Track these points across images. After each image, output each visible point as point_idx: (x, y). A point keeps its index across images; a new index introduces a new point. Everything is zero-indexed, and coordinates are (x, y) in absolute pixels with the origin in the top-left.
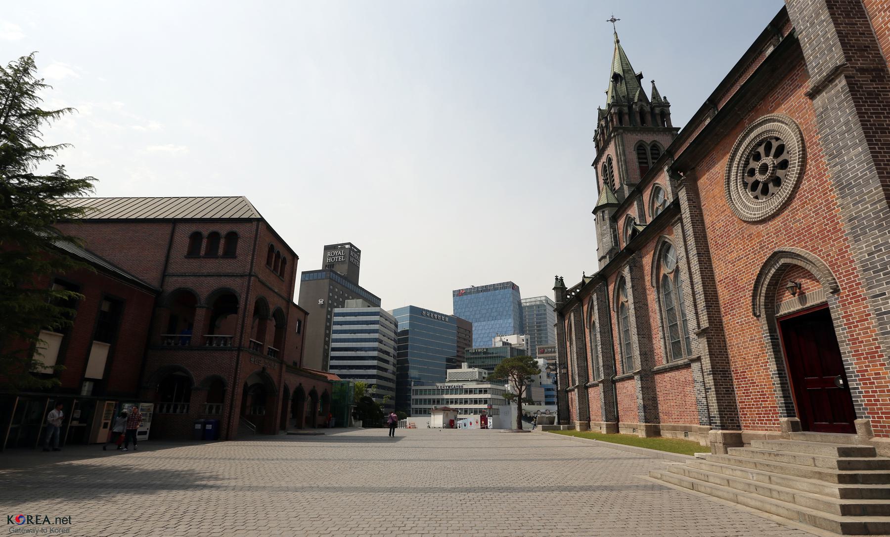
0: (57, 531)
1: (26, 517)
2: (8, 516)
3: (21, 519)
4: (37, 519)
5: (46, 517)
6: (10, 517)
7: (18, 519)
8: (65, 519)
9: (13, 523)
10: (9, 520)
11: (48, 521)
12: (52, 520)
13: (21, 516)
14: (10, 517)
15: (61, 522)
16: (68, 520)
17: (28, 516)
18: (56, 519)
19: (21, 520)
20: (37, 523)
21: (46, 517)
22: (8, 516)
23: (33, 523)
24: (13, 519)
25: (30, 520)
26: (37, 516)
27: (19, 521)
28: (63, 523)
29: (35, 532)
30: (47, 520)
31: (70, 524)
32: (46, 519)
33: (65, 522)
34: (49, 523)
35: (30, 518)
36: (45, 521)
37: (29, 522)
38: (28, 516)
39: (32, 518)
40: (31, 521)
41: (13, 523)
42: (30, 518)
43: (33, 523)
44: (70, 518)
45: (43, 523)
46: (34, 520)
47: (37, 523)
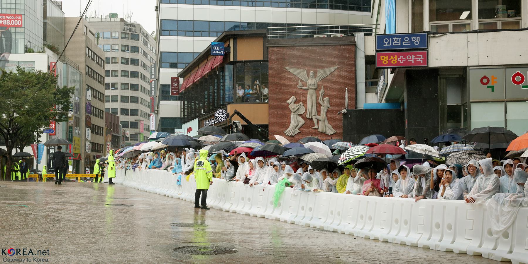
0: (38, 260)
2: (2, 249)
3: (11, 251)
4: (24, 252)
5: (31, 250)
6: (4, 250)
7: (9, 252)
9: (6, 255)
10: (3, 252)
11: (32, 252)
12: (35, 252)
13: (12, 249)
14: (4, 250)
15: (42, 254)
16: (47, 252)
18: (38, 251)
19: (12, 252)
20: (24, 254)
21: (31, 250)
22: (2, 249)
23: (21, 255)
24: (6, 251)
27: (10, 253)
28: (43, 255)
29: (23, 261)
32: (31, 252)
33: (44, 254)
34: (33, 255)
35: (18, 250)
36: (30, 252)
37: (18, 254)
38: (17, 249)
39: (20, 250)
41: (6, 255)
42: (18, 250)
44: (48, 251)
45: (28, 255)
46: (21, 252)
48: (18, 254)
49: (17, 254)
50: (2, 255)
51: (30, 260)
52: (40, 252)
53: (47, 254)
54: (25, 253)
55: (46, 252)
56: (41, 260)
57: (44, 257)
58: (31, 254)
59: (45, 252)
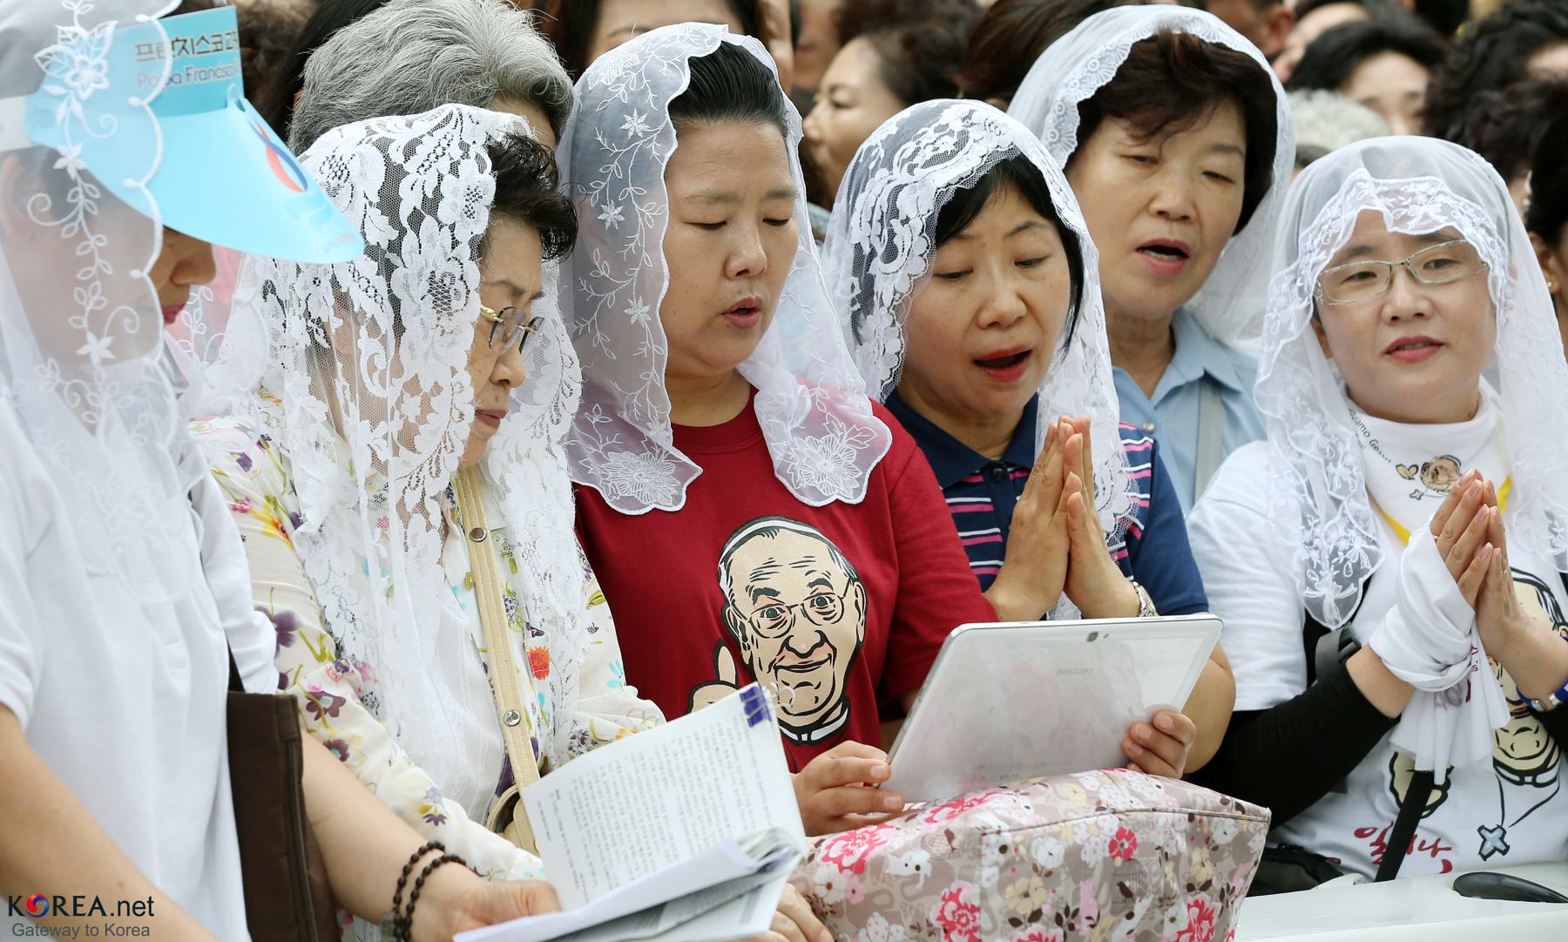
0: (120, 931)
1: (52, 901)
2: (11, 898)
4: (76, 905)
5: (97, 900)
7: (32, 905)
8: (137, 906)
11: (101, 908)
12: (110, 907)
17: (55, 898)
18: (120, 904)
19: (41, 905)
20: (75, 914)
21: (97, 900)
22: (11, 898)
23: (66, 914)
24: (22, 905)
25: (59, 907)
26: (75, 898)
27: (34, 909)
30: (97, 904)
31: (152, 915)
32: (97, 905)
34: (104, 914)
35: (59, 901)
36: (93, 908)
37: (58, 910)
38: (55, 898)
41: (21, 914)
43: (66, 914)
45: (90, 914)
46: (69, 907)
47: (75, 914)
48: (58, 910)
49: (55, 914)
50: (11, 914)
51: (94, 931)
52: (124, 906)
55: (144, 908)
56: (130, 930)
57: (140, 922)
58: (97, 912)
59: (141, 905)
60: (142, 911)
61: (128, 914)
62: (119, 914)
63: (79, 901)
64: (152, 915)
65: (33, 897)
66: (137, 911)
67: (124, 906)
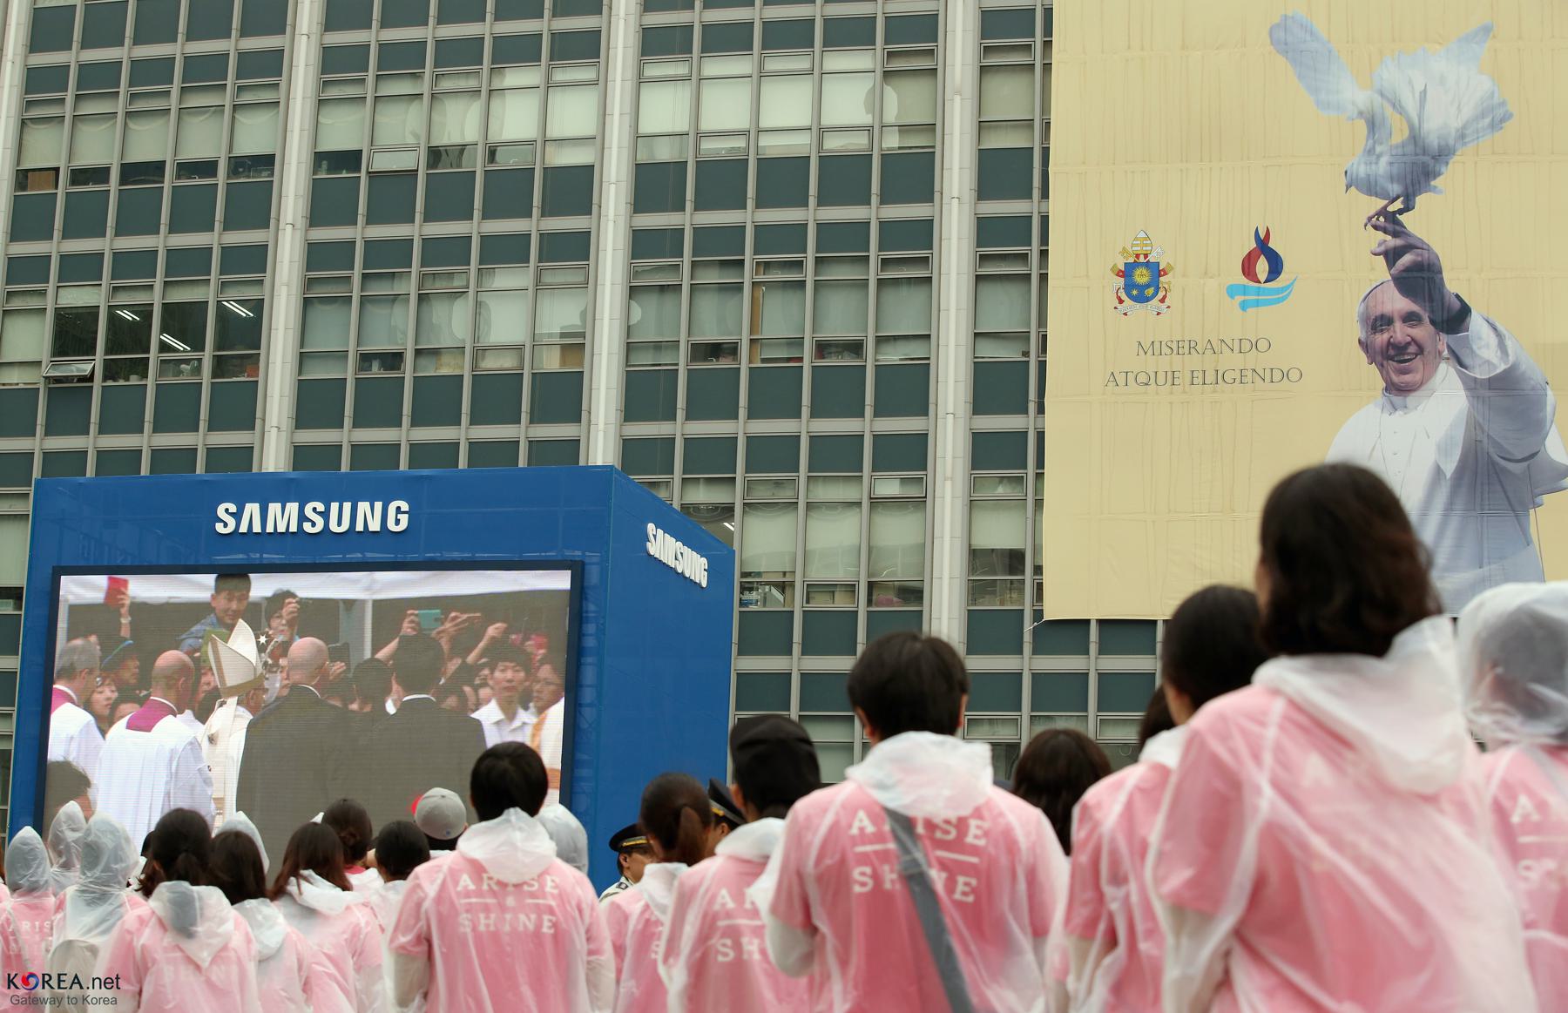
0: (94, 1001)
2: (9, 975)
4: (59, 981)
5: (76, 977)
8: (107, 981)
9: (17, 988)
11: (79, 983)
13: (32, 975)
17: (44, 975)
18: (94, 980)
19: (32, 981)
20: (59, 988)
21: (76, 977)
22: (9, 975)
23: (52, 988)
24: (18, 981)
25: (47, 982)
26: (59, 975)
28: (105, 987)
29: (57, 1002)
31: (118, 988)
32: (76, 981)
33: (107, 985)
34: (81, 988)
35: (47, 978)
36: (73, 983)
37: (46, 985)
38: (44, 975)
39: (50, 978)
40: (49, 984)
41: (17, 988)
42: (47, 978)
44: (117, 978)
45: (71, 988)
46: (54, 983)
47: (59, 988)
48: (46, 985)
49: (44, 988)
50: (9, 988)
52: (97, 982)
53: (115, 986)
54: (62, 983)
55: (113, 982)
56: (102, 1000)
58: (76, 986)
60: (111, 985)
61: (100, 988)
62: (93, 988)
63: (62, 978)
64: (118, 988)
65: (27, 975)
66: (107, 985)
67: (97, 982)
